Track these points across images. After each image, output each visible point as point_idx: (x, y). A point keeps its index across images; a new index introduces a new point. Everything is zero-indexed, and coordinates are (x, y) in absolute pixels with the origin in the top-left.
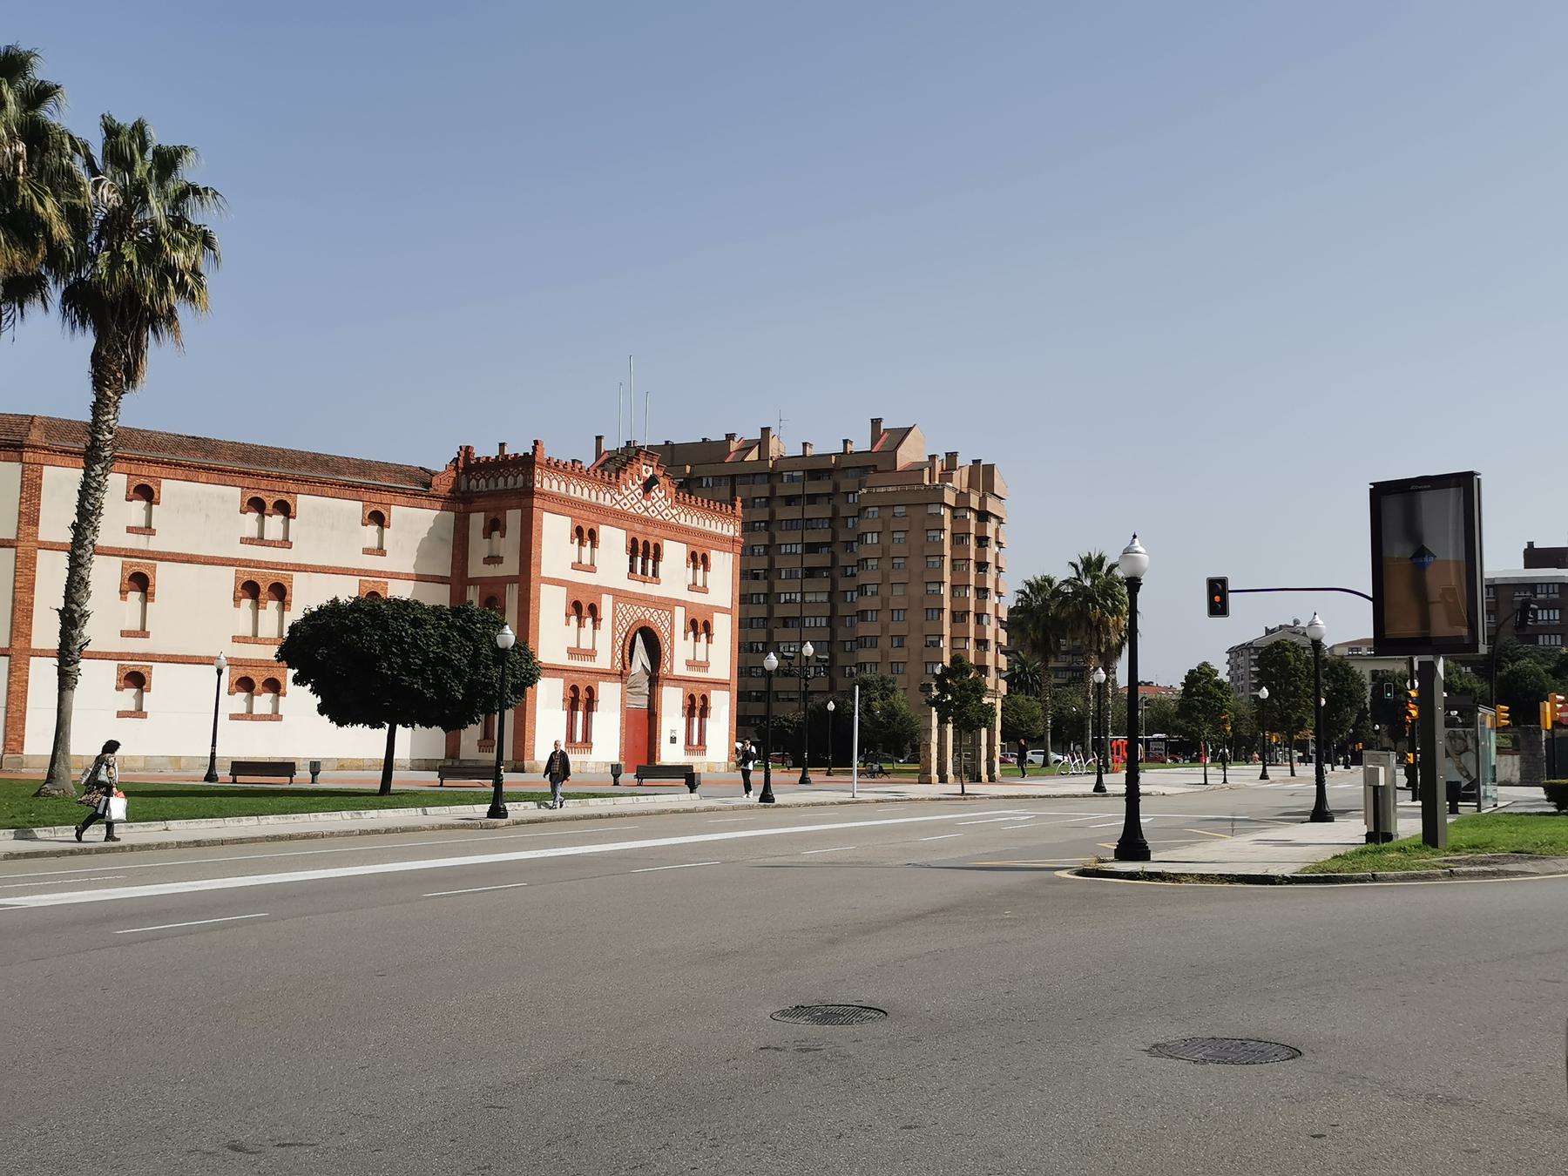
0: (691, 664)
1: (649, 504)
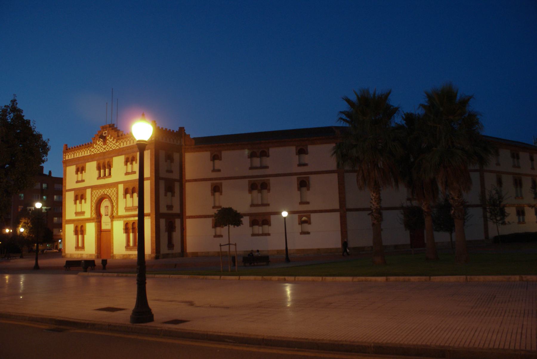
1: (106, 146)
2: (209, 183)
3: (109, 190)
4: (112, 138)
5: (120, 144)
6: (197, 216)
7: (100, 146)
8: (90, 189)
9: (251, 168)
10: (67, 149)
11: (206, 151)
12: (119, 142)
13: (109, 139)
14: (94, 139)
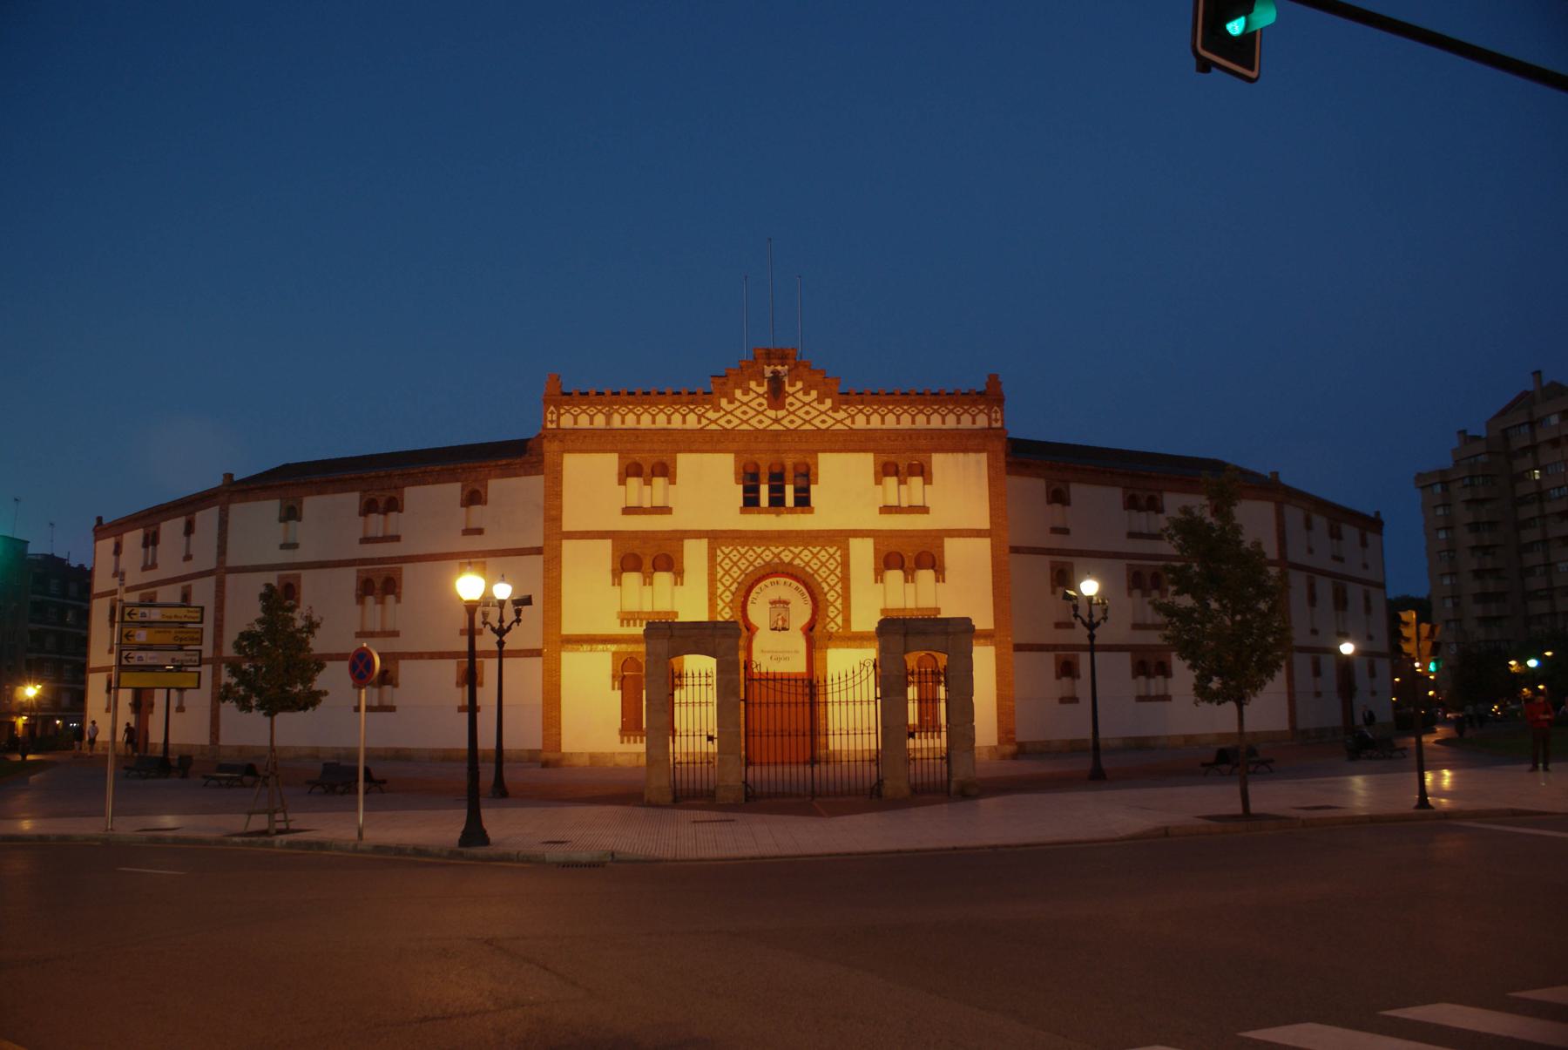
1: (781, 413)
5: (852, 417)
8: (704, 543)
11: (1039, 476)
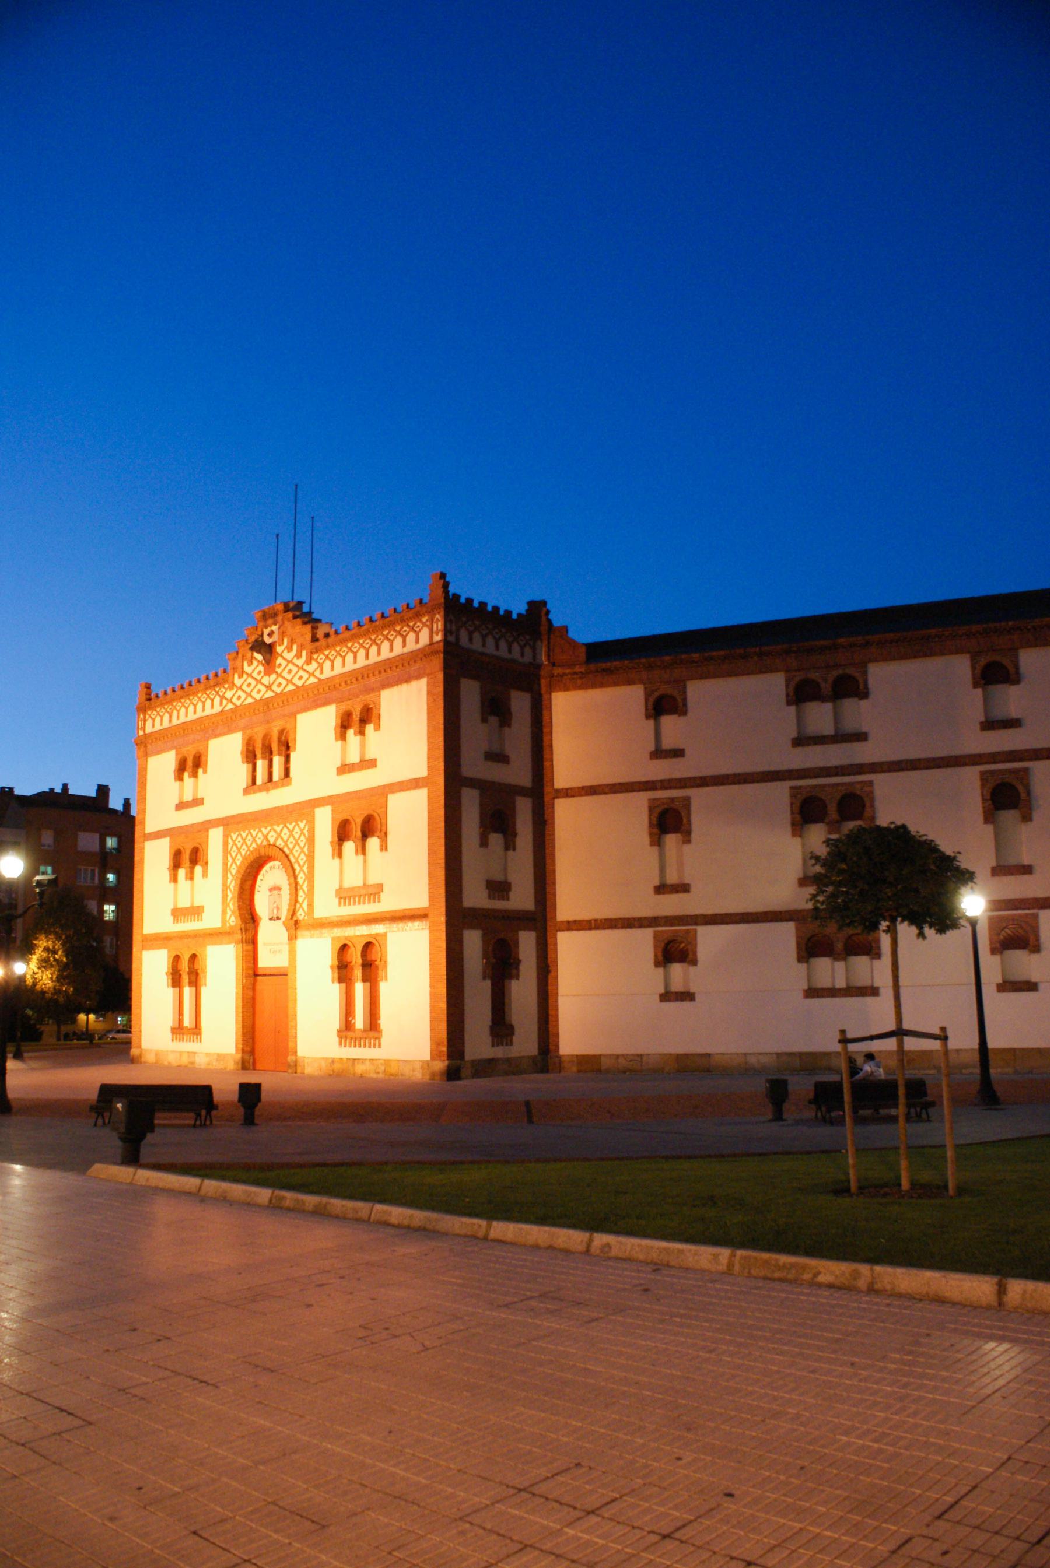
0: (345, 895)
1: (273, 676)
2: (641, 801)
3: (281, 831)
4: (295, 647)
5: (321, 666)
6: (596, 920)
7: (255, 679)
9: (799, 741)
10: (149, 700)
11: (630, 682)
12: (316, 660)
13: (286, 654)
14: (235, 658)
